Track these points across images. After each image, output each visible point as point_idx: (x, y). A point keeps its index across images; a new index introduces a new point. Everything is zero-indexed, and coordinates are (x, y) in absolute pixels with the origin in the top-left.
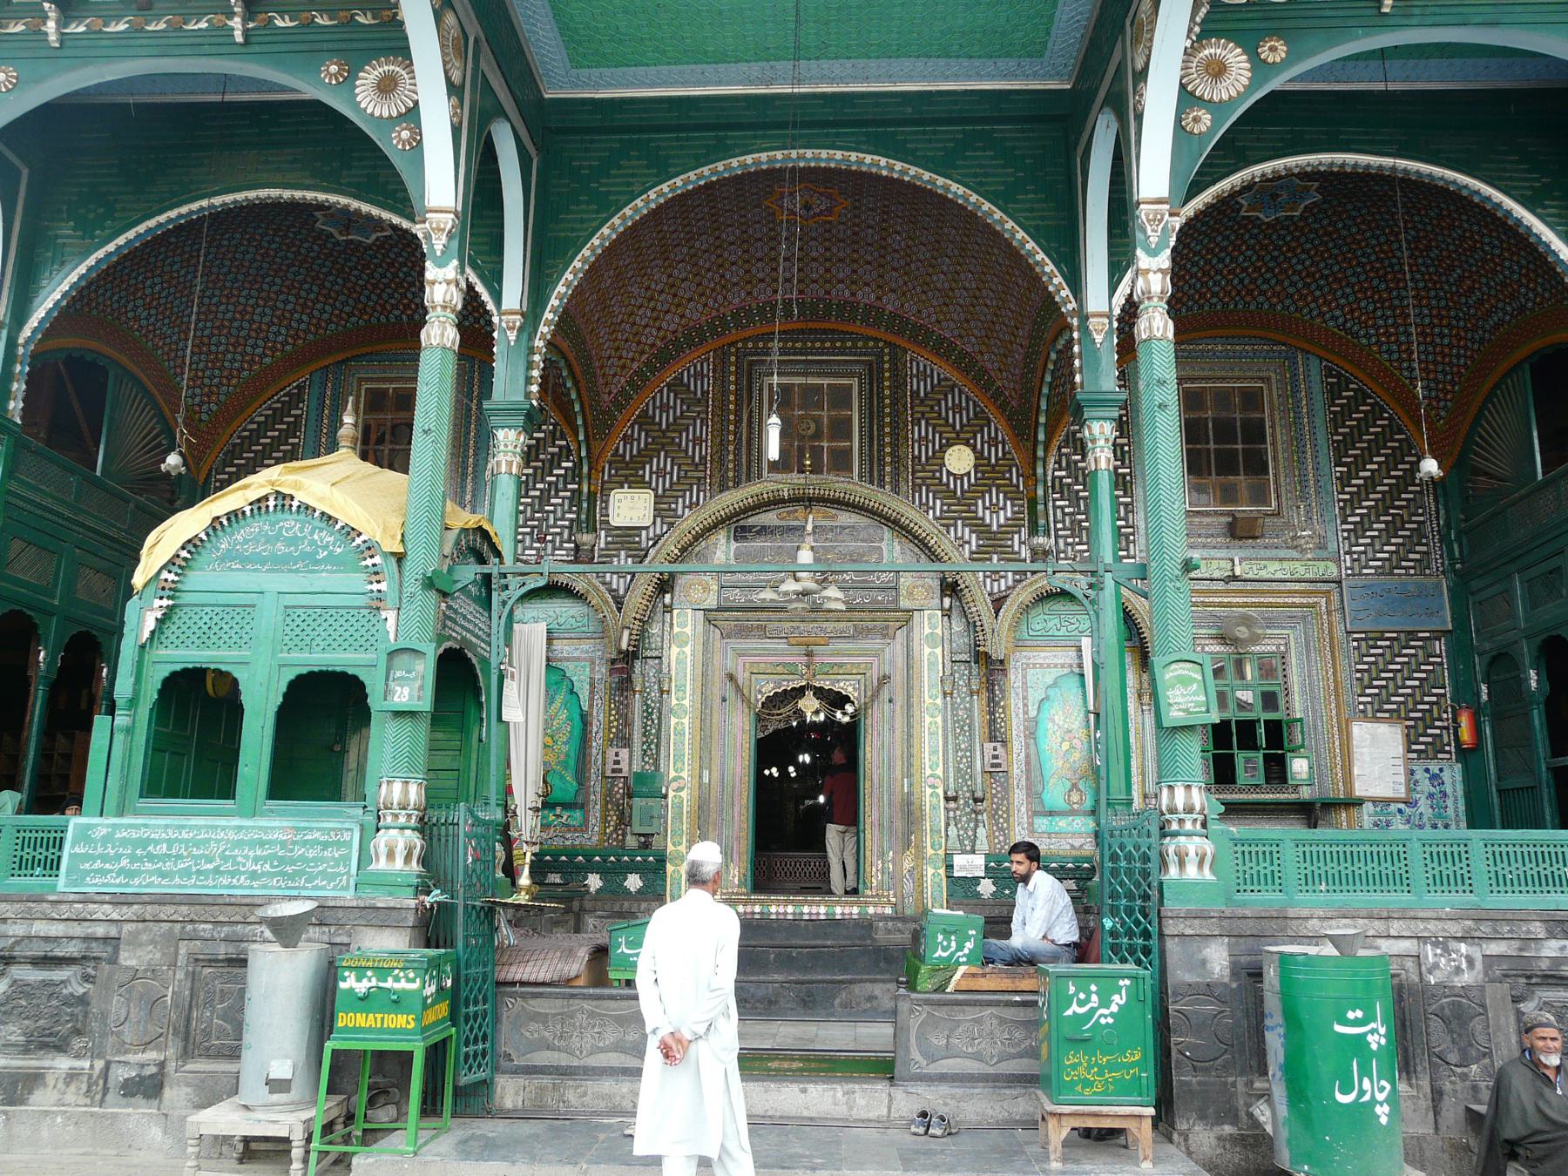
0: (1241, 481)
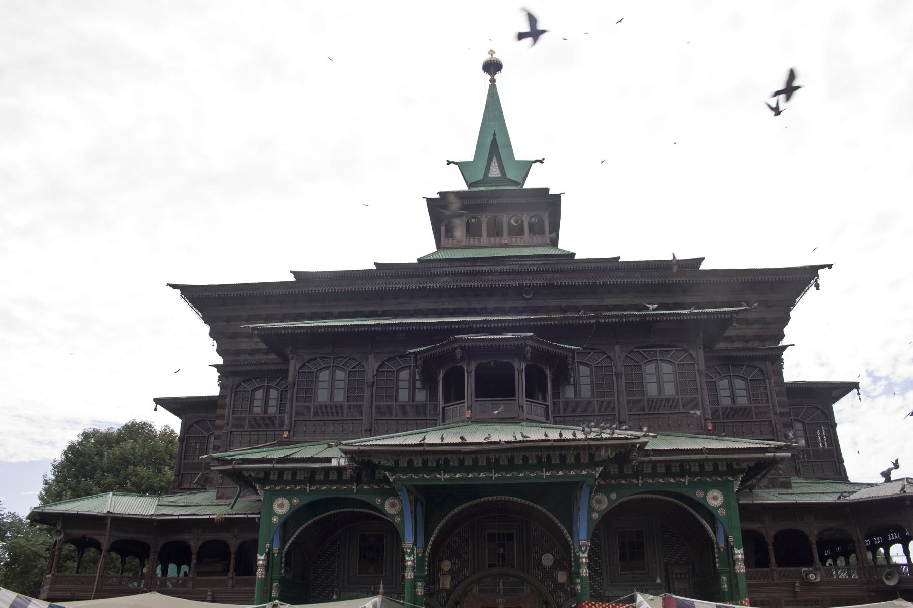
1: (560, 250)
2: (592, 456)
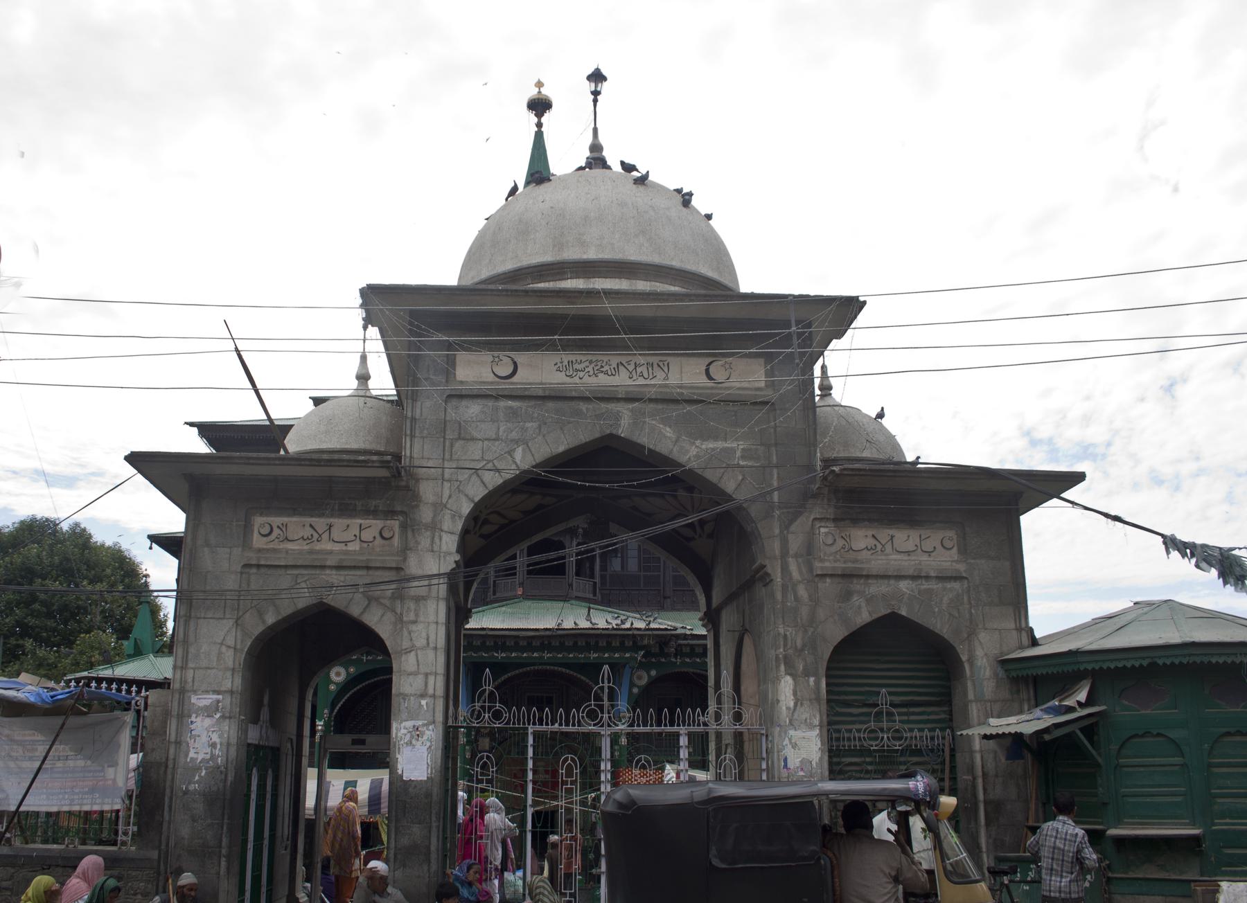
2: (634, 642)
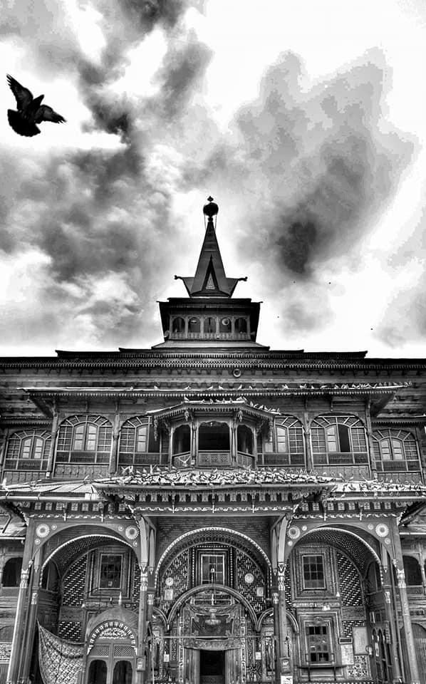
0: (317, 581)
1: (258, 344)
2: (290, 496)
